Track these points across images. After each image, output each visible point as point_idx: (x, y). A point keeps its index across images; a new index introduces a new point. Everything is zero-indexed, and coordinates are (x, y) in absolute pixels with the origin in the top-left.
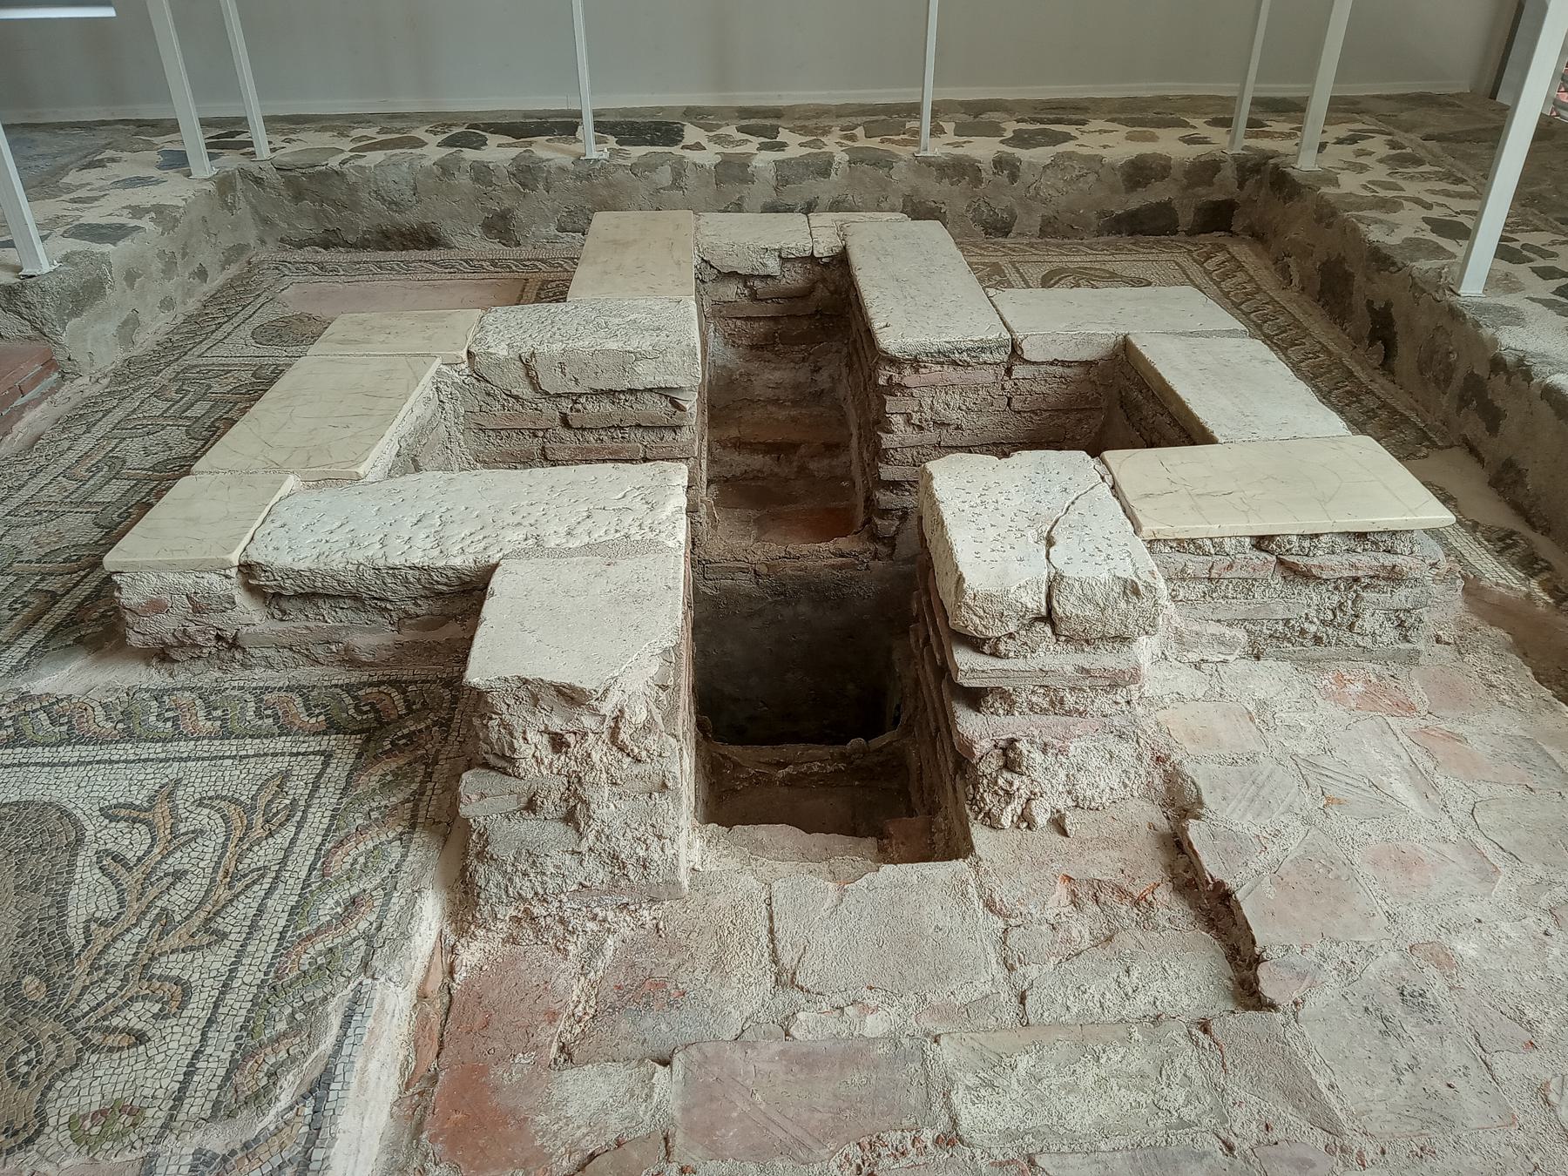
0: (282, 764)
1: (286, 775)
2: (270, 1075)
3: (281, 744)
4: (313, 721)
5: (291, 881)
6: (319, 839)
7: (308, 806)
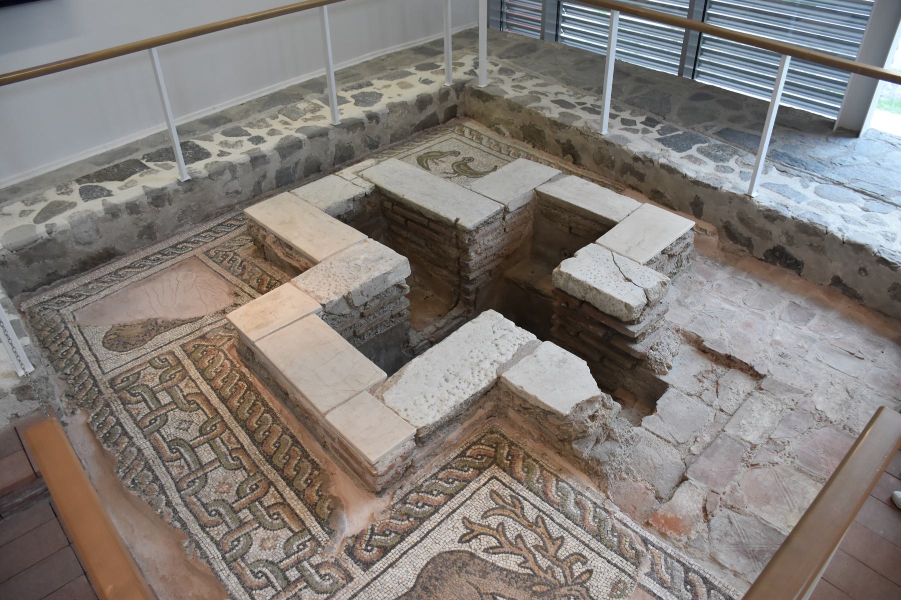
0: (485, 490)
2: (633, 548)
7: (518, 494)
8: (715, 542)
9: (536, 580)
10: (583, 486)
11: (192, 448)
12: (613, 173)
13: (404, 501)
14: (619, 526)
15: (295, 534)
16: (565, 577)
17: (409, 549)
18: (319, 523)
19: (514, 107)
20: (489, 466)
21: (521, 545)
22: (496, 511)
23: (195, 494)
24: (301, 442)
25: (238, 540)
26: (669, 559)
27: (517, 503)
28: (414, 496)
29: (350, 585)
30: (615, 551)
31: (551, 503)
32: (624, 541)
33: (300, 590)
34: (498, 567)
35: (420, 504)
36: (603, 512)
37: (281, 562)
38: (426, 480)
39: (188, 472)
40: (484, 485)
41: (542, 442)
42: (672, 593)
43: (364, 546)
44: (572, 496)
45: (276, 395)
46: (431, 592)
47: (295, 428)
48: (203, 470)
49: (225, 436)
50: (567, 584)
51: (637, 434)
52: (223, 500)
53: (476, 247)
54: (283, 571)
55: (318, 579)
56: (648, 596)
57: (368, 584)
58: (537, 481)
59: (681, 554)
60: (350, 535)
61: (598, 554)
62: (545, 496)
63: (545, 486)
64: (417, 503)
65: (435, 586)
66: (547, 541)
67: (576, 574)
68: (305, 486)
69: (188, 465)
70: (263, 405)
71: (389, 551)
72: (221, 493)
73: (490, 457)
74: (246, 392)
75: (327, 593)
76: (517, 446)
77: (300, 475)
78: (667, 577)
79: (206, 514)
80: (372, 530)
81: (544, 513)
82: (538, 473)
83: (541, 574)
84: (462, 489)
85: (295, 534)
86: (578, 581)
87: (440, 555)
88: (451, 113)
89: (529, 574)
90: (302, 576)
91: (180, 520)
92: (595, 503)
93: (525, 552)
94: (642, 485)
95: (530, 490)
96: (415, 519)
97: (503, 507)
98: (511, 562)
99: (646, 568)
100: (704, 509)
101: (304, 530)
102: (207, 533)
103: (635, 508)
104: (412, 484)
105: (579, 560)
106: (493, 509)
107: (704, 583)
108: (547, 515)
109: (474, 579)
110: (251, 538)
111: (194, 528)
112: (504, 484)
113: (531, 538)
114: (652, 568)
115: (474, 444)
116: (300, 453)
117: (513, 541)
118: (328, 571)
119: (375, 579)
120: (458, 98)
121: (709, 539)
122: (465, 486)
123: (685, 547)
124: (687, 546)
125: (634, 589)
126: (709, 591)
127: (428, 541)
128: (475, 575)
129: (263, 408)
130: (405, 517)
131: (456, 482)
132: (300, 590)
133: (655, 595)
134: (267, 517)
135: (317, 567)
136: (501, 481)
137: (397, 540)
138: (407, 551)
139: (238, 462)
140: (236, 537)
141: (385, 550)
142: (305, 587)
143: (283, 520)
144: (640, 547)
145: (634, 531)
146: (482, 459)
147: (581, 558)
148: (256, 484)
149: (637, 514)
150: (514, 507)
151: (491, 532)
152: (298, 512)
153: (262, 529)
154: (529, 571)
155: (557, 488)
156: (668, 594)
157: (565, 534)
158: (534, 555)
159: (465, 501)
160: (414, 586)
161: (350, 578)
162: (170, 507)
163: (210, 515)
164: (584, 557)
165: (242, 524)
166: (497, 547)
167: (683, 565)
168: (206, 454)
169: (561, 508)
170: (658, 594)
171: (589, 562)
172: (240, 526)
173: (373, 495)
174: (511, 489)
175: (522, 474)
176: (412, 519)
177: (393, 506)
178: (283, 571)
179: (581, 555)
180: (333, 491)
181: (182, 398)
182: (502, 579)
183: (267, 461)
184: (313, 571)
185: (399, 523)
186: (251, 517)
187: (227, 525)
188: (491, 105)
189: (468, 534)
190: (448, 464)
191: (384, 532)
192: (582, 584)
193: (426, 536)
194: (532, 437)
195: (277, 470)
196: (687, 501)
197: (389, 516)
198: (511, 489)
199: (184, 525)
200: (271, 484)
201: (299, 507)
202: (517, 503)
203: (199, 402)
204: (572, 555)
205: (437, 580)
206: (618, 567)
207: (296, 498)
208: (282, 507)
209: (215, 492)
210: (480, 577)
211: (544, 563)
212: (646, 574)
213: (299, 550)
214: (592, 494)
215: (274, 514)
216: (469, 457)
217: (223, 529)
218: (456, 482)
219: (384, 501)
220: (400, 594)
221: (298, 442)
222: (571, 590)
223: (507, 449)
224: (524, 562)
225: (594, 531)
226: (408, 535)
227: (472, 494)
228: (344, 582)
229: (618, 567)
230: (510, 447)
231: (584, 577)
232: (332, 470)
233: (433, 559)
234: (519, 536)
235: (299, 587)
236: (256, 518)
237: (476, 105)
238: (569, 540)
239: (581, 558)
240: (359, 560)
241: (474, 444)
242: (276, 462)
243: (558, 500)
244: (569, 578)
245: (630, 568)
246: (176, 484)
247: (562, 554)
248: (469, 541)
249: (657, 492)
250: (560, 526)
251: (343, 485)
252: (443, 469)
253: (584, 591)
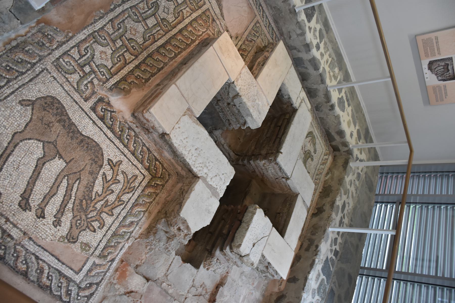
0: (137, 172)
2: (108, 254)
7: (136, 190)
8: (113, 299)
9: (89, 202)
10: (142, 225)
11: (154, 15)
12: (309, 235)
13: (130, 128)
14: (120, 246)
15: (110, 70)
16: (91, 217)
17: (103, 132)
18: (116, 83)
19: (341, 181)
20: (150, 174)
21: (108, 193)
22: (126, 178)
23: (129, 16)
24: (160, 73)
25: (105, 39)
26: (103, 274)
27: (131, 190)
28: (133, 134)
29: (82, 100)
30: (106, 244)
31: (132, 208)
32: (112, 249)
33: (79, 73)
34: (95, 181)
35: (128, 137)
36: (127, 237)
37: (94, 62)
38: (141, 140)
39: (141, 12)
40: (140, 172)
41: (165, 202)
42: (84, 276)
43: (104, 107)
44: (136, 220)
45: (184, 59)
46: (80, 145)
47: (167, 69)
48: (143, 21)
49: (161, 32)
50: (87, 218)
51: (171, 253)
52: (126, 31)
53: (268, 164)
54: (89, 64)
55: (85, 82)
56: (82, 263)
57: (83, 110)
58: (143, 201)
59: (106, 280)
60: (110, 100)
61: (105, 235)
62: (135, 205)
63: (141, 205)
64: (129, 135)
65: (83, 146)
66: (110, 207)
67: (93, 224)
68: (136, 75)
69: (145, 13)
70: (179, 52)
71: (102, 121)
72: (130, 30)
73: (155, 175)
74: (185, 43)
75: (78, 87)
76: (162, 189)
77: (141, 72)
78: (93, 273)
79: (118, 22)
80: (113, 112)
81: (126, 205)
82: (148, 201)
83: (92, 204)
84: (137, 160)
85: (110, 70)
86: (89, 225)
87: (101, 149)
88: (335, 149)
89: (92, 197)
90: (86, 74)
91: (115, 8)
92: (132, 232)
93: (104, 195)
94: (144, 257)
95: (138, 197)
96: (120, 135)
97: (128, 182)
98: (98, 187)
99: (98, 261)
100: (132, 292)
101: (112, 75)
102: (108, 23)
103: (131, 254)
104: (139, 132)
105: (101, 225)
106: (127, 177)
107: (91, 294)
108: (125, 206)
109: (88, 167)
110: (106, 46)
111: (111, 16)
112: (141, 182)
113: (112, 198)
114: (98, 265)
115: (162, 166)
116: (154, 72)
117: (110, 188)
118: (90, 88)
119: (86, 114)
120: (344, 152)
121: (115, 295)
122: (139, 161)
123: (110, 282)
124: (111, 283)
125: (86, 255)
126: (86, 296)
127: (108, 142)
128: (90, 168)
129: (177, 52)
130: (121, 129)
131: (141, 157)
132: (79, 73)
133: (83, 267)
134: (118, 55)
135: (91, 82)
136: (142, 181)
137: (108, 125)
138: (102, 131)
139: (147, 39)
140: (107, 38)
141: (102, 119)
142: (80, 76)
143: (117, 63)
144: (109, 258)
145: (118, 254)
146: (155, 170)
147: (102, 225)
148: (136, 48)
149: (128, 255)
150: (129, 188)
151: (114, 176)
152: (122, 71)
153: (112, 52)
154: (94, 197)
155: (140, 211)
156: (84, 274)
157: (115, 217)
158: (102, 200)
159: (131, 162)
160: (83, 135)
161: (86, 100)
162: (122, 3)
163: (118, 24)
164: (103, 227)
165: (114, 41)
166: (106, 180)
167: (100, 282)
168: (151, 22)
169: (129, 214)
170: (84, 269)
171: (100, 230)
172: (113, 40)
173: (132, 112)
174: (139, 186)
175: (147, 192)
176: (120, 133)
177: (126, 123)
178: (89, 64)
179: (104, 225)
180: (134, 90)
181: (181, 9)
182: (88, 183)
183: (149, 54)
184: (89, 80)
185: (118, 126)
186: (118, 46)
187: (113, 34)
188: (341, 169)
189: (113, 163)
190: (151, 152)
191: (112, 118)
192: (87, 227)
193: (111, 141)
194: (167, 197)
195: (144, 60)
196: (136, 282)
197: (121, 120)
198: (139, 186)
199: (112, 10)
200: (137, 57)
201: (124, 72)
202: (131, 190)
203: (179, 18)
204: (103, 221)
205: (87, 147)
206: (98, 246)
207: (129, 70)
208: (124, 62)
209: (131, 27)
210: (89, 171)
211: (98, 206)
212: (94, 262)
213: (101, 72)
214: (137, 231)
215: (120, 59)
216: (155, 163)
217: (111, 31)
218: (141, 157)
219: (129, 118)
220: (78, 127)
221: (159, 71)
222: (84, 221)
223: (160, 184)
224: (98, 195)
225: (117, 233)
226: (111, 131)
227: (135, 165)
228: (84, 97)
229: (98, 246)
230: (161, 185)
231: (91, 228)
232: (145, 90)
233: (98, 145)
234: (113, 192)
235: (80, 73)
236: (117, 49)
237: (340, 161)
238: (112, 219)
239: (102, 225)
240: (96, 105)
241: (162, 166)
242: (148, 59)
243: (134, 212)
244: (91, 219)
245: (97, 252)
246: (134, 6)
247: (104, 215)
248: (109, 164)
249: (140, 265)
250: (119, 214)
251: (137, 95)
252: (148, 149)
253: (83, 228)
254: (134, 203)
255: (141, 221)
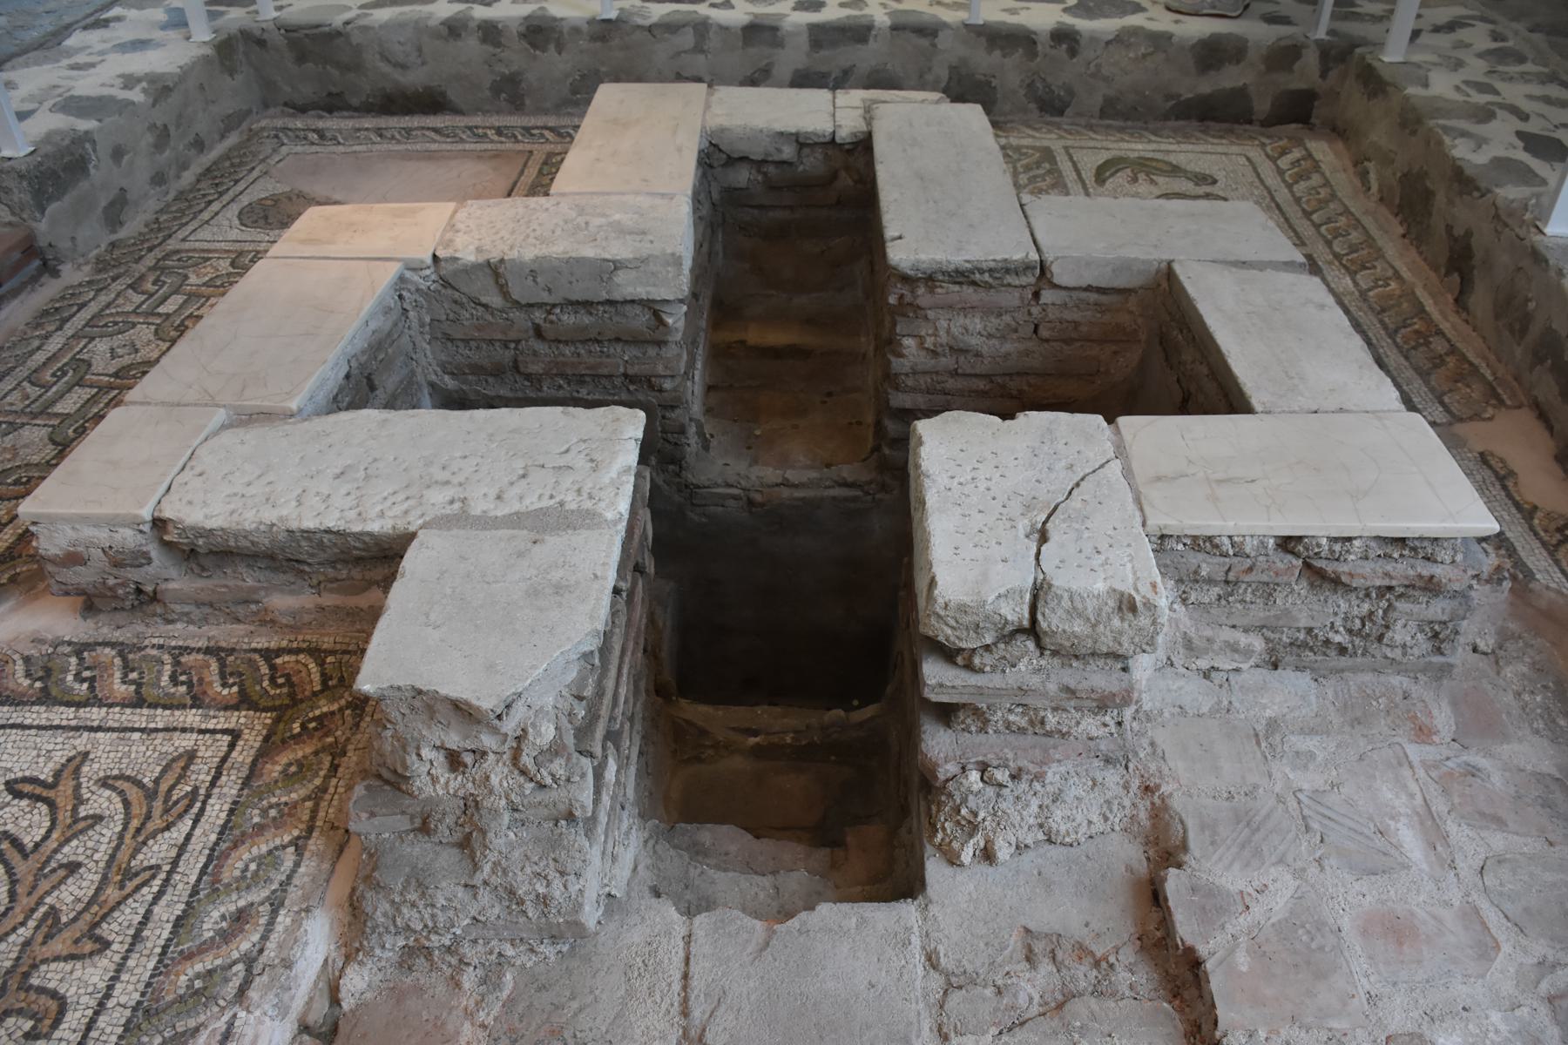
0: (185, 742)
1: (191, 756)
3: (192, 717)
4: (225, 692)
5: (180, 886)
6: (213, 837)
7: (208, 796)
95: (231, 812)
175: (274, 770)
254: (216, 844)
255: (296, 881)
